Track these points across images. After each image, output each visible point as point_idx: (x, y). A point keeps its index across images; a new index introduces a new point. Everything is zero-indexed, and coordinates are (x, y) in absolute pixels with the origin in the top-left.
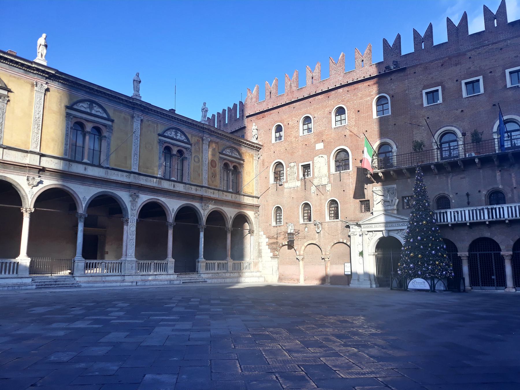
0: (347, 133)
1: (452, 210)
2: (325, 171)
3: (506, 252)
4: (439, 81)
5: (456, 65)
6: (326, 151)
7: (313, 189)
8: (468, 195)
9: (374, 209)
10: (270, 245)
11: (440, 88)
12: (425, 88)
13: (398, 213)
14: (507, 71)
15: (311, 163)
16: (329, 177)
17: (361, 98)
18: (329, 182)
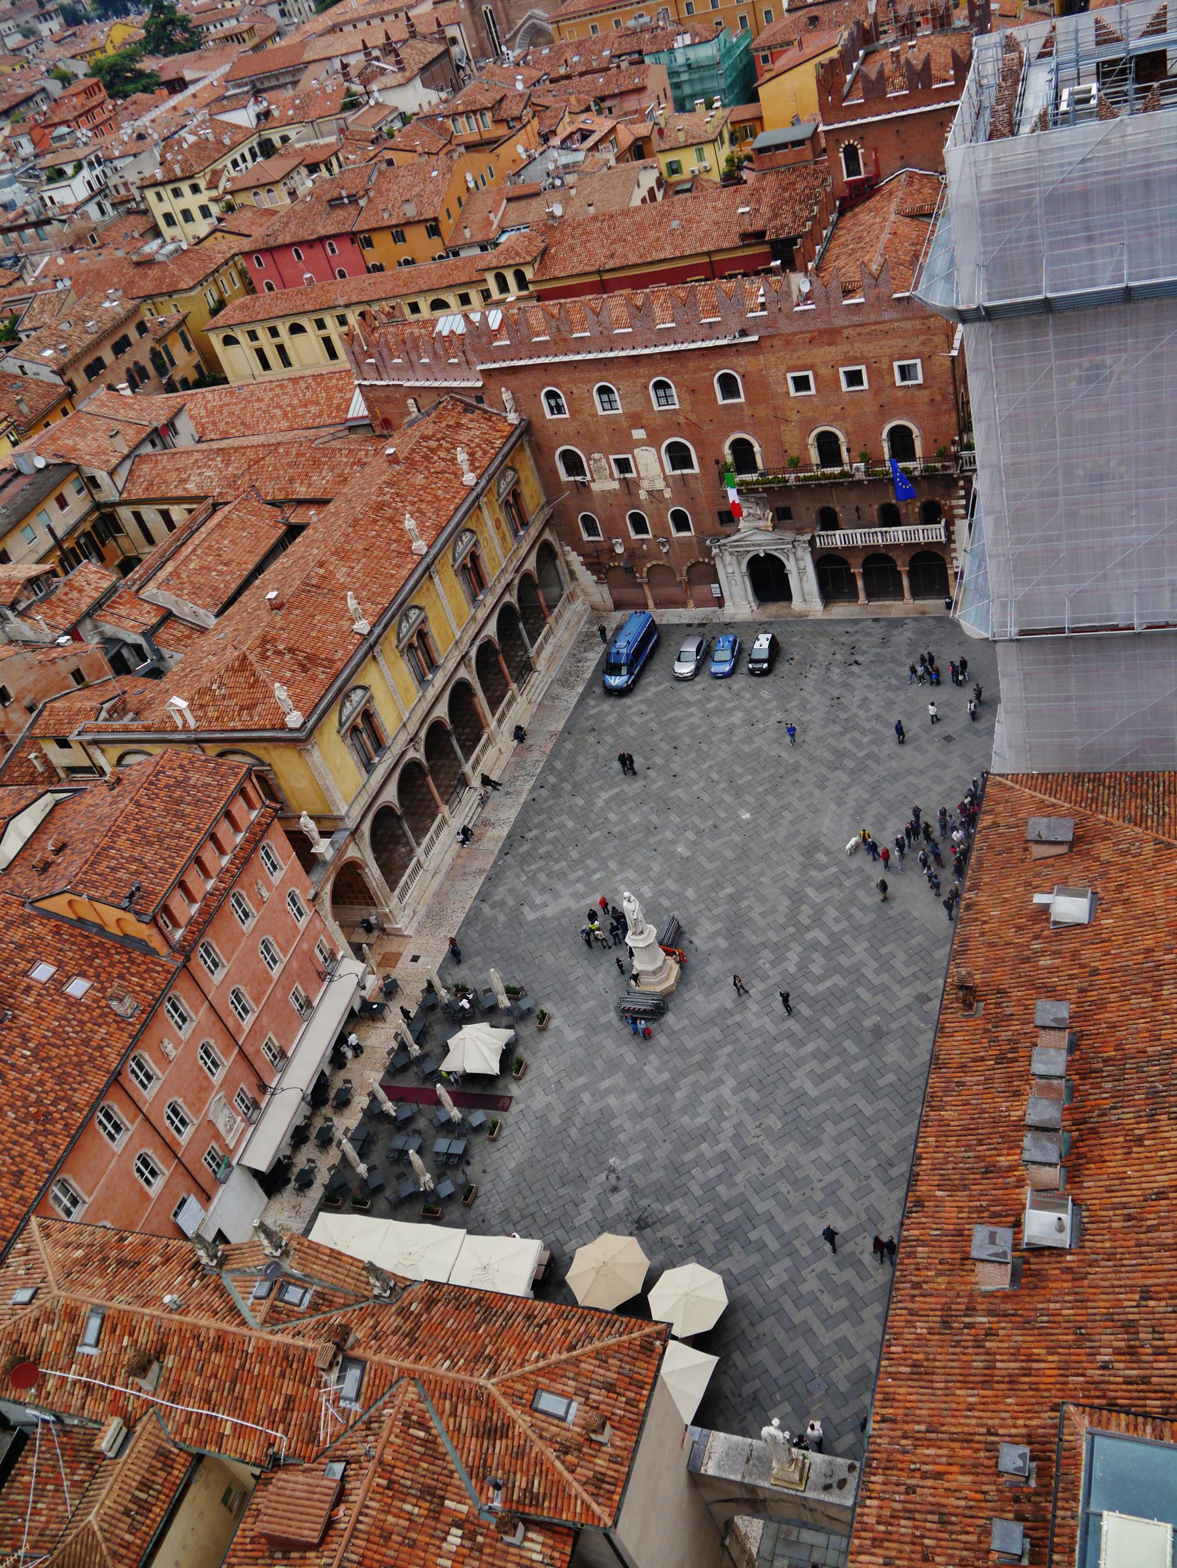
0: (682, 420)
1: (841, 532)
2: (658, 470)
3: (903, 569)
4: (808, 361)
5: (830, 344)
6: (653, 440)
7: (643, 495)
8: (857, 509)
9: (742, 524)
10: (588, 565)
11: (810, 373)
12: (790, 370)
13: (774, 528)
14: (896, 364)
15: (629, 456)
16: (665, 478)
17: (694, 372)
18: (667, 486)
